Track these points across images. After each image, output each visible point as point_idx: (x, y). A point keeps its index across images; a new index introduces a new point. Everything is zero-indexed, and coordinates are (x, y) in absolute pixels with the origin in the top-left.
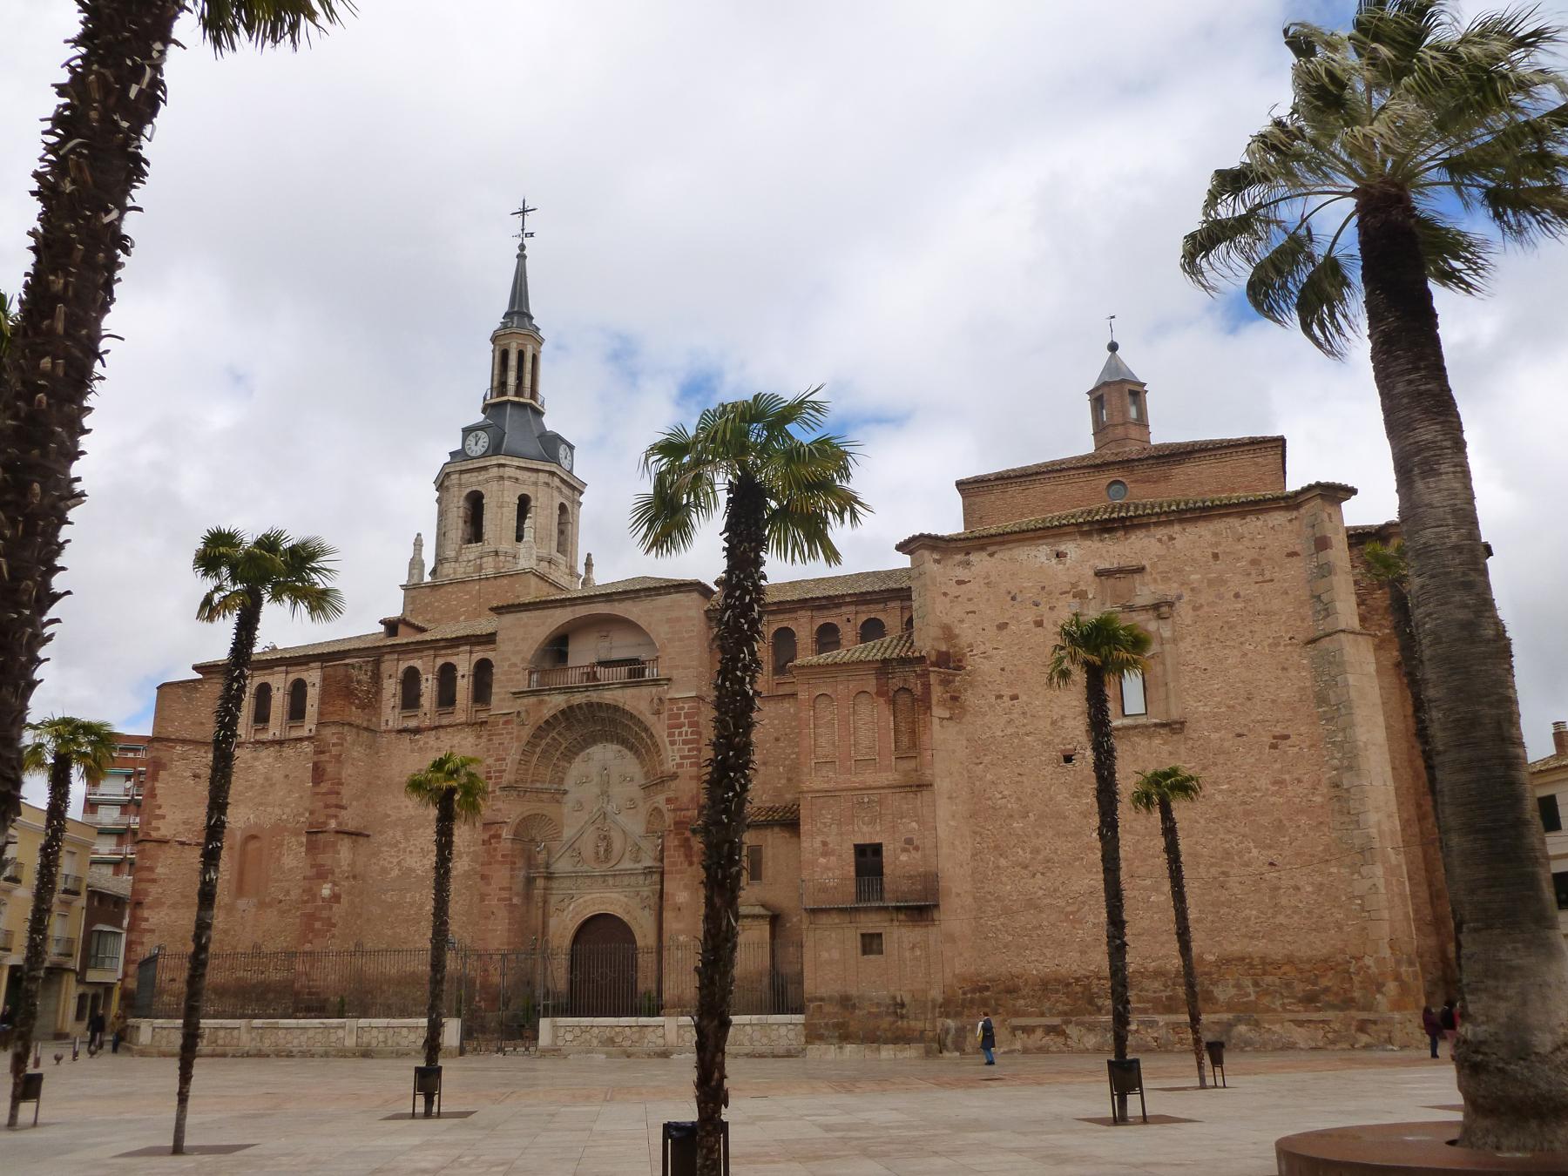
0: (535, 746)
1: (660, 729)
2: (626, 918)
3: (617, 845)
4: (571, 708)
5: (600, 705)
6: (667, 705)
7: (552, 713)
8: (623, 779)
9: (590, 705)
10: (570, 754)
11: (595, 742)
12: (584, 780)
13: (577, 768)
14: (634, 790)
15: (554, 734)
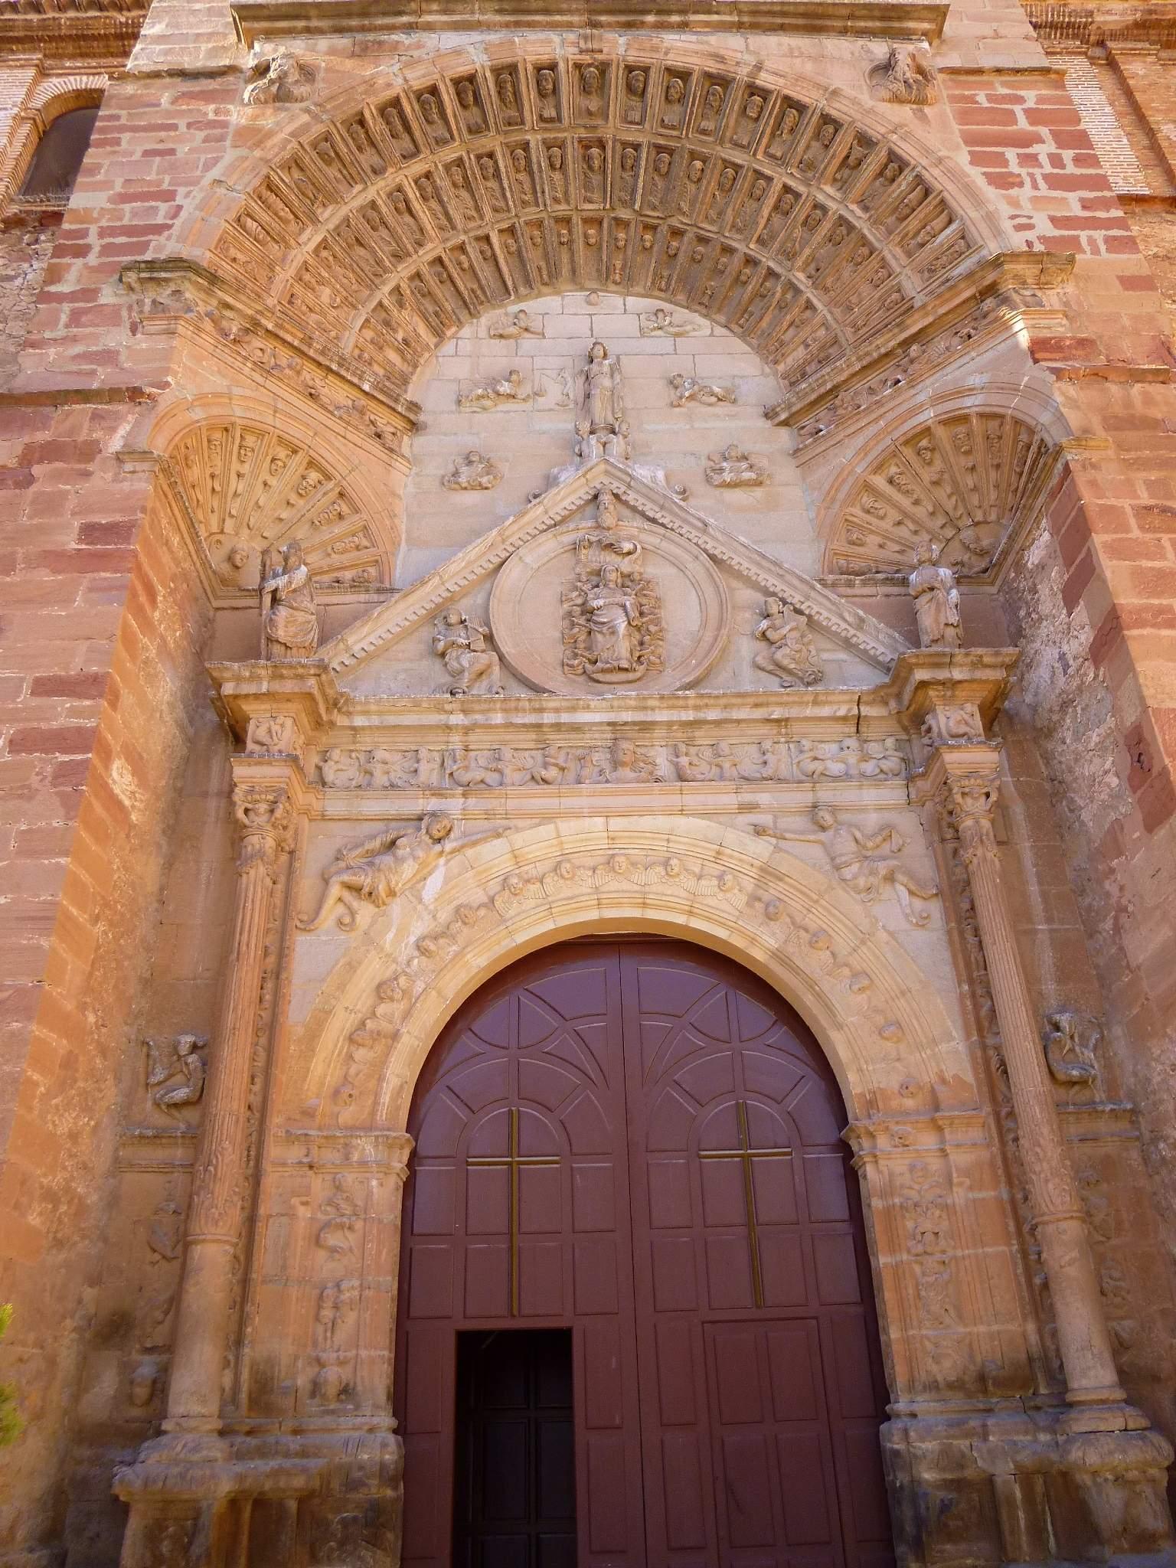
0: (319, 194)
1: (934, 140)
2: (757, 943)
3: (683, 613)
4: (506, 72)
5: (636, 79)
6: (940, 88)
7: (418, 78)
8: (683, 391)
9: (593, 77)
10: (457, 292)
11: (551, 278)
12: (495, 389)
13: (468, 351)
14: (747, 429)
15: (405, 175)
